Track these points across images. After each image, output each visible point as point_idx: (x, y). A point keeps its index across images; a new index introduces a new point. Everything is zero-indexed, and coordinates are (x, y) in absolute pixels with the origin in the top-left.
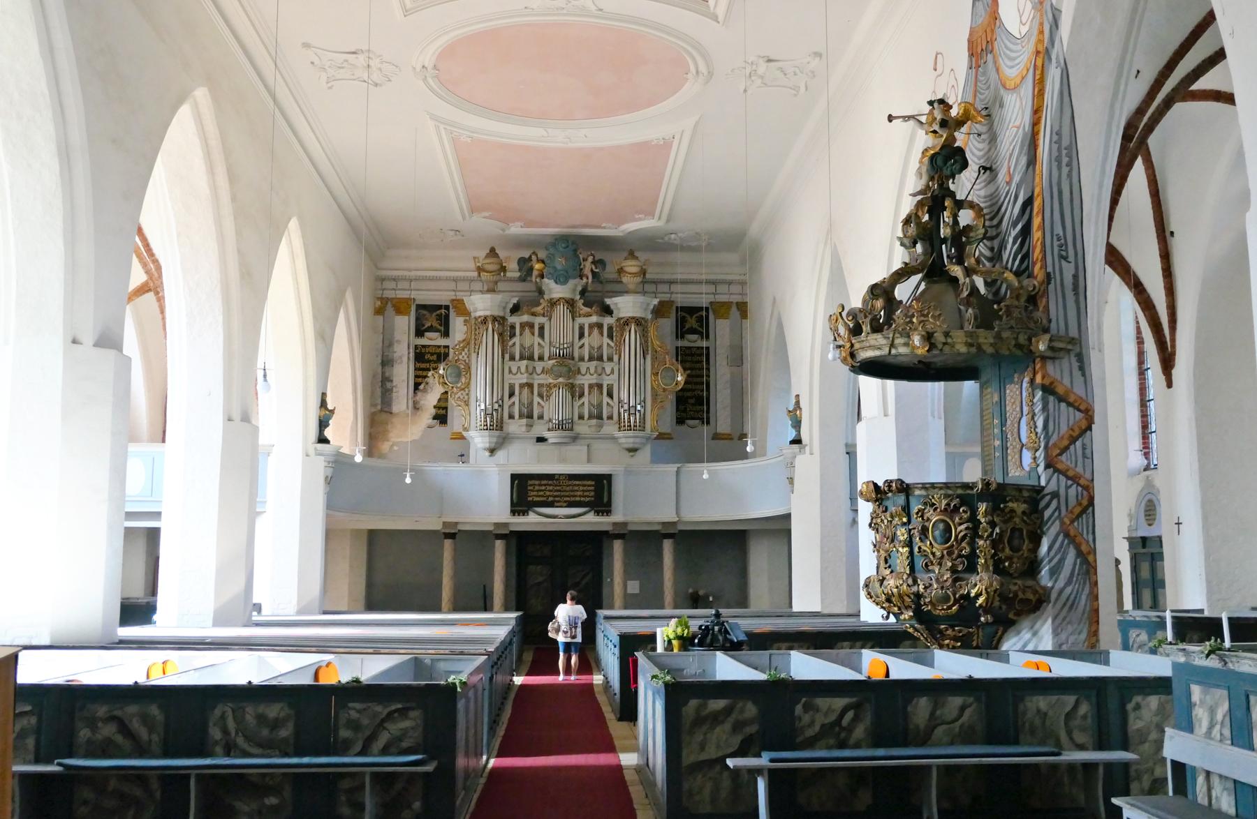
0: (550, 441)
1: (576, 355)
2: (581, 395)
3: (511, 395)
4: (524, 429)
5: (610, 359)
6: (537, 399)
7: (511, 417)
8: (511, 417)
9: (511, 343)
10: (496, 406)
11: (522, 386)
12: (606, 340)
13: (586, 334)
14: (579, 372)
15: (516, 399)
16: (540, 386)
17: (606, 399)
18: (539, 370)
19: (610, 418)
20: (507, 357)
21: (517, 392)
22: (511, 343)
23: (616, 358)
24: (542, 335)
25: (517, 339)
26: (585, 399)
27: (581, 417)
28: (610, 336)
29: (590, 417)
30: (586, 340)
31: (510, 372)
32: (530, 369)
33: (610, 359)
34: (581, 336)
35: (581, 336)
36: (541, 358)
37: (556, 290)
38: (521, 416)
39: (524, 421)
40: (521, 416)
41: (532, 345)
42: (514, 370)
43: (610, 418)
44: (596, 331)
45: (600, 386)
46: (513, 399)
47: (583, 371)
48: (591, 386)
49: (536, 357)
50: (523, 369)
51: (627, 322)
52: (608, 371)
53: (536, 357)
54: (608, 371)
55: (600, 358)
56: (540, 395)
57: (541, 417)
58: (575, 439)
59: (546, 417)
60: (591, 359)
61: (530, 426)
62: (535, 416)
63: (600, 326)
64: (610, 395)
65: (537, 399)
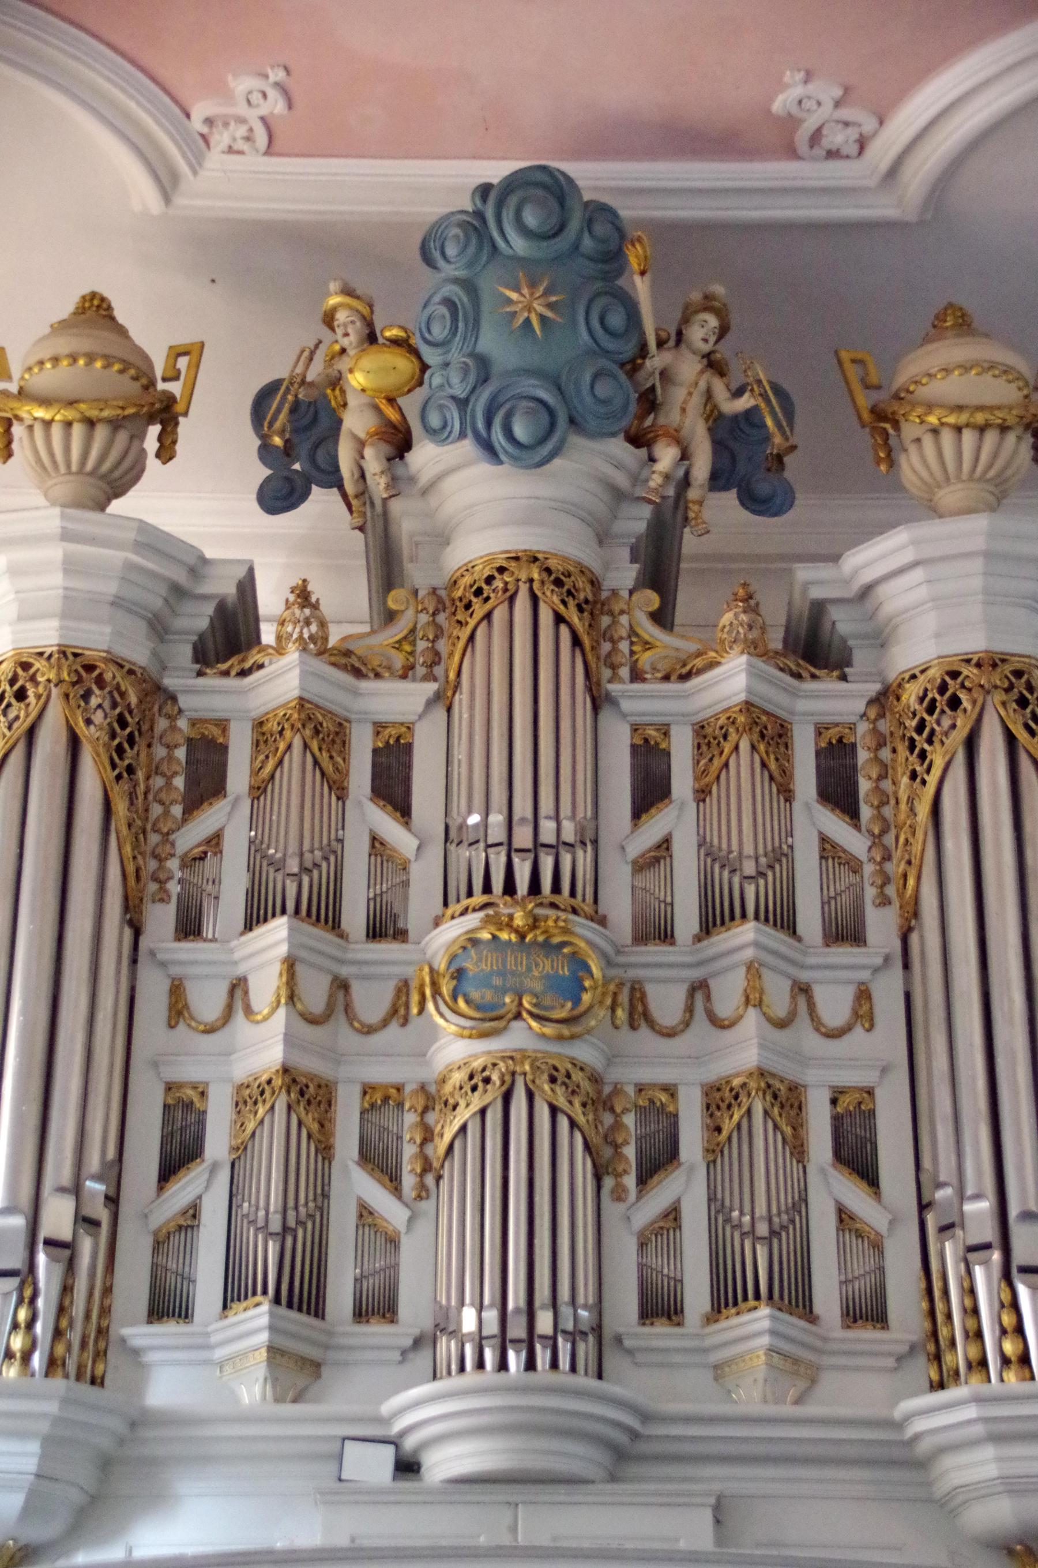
0: (444, 1463)
1: (619, 903)
2: (659, 1158)
3: (179, 1155)
4: (251, 1388)
5: (846, 931)
6: (355, 1184)
7: (167, 1305)
8: (167, 1305)
9: (190, 837)
10: (58, 1217)
11: (248, 1097)
12: (813, 820)
13: (682, 781)
14: (639, 1014)
15: (204, 1187)
16: (380, 1100)
17: (830, 1187)
18: (371, 1001)
19: (868, 1311)
20: (161, 919)
21: (217, 1143)
22: (190, 837)
23: (881, 926)
24: (393, 788)
25: (229, 818)
26: (687, 1187)
27: (660, 1305)
28: (839, 793)
29: (727, 1296)
30: (677, 820)
31: (178, 1009)
32: (315, 992)
33: (846, 931)
34: (650, 791)
35: (650, 791)
36: (384, 927)
37: (481, 508)
38: (235, 1292)
39: (257, 1317)
40: (235, 1292)
41: (334, 851)
42: (206, 1001)
43: (868, 1311)
44: (744, 762)
45: (787, 1100)
46: (186, 1188)
47: (667, 1002)
48: (719, 1099)
49: (355, 916)
50: (266, 985)
51: (948, 692)
52: (834, 1003)
53: (355, 916)
54: (834, 1003)
55: (783, 919)
56: (379, 1161)
57: (377, 1305)
58: (627, 1453)
59: (414, 1309)
60: (715, 917)
61: (298, 1369)
62: (340, 1295)
63: (770, 732)
64: (858, 1159)
65: (355, 1184)
